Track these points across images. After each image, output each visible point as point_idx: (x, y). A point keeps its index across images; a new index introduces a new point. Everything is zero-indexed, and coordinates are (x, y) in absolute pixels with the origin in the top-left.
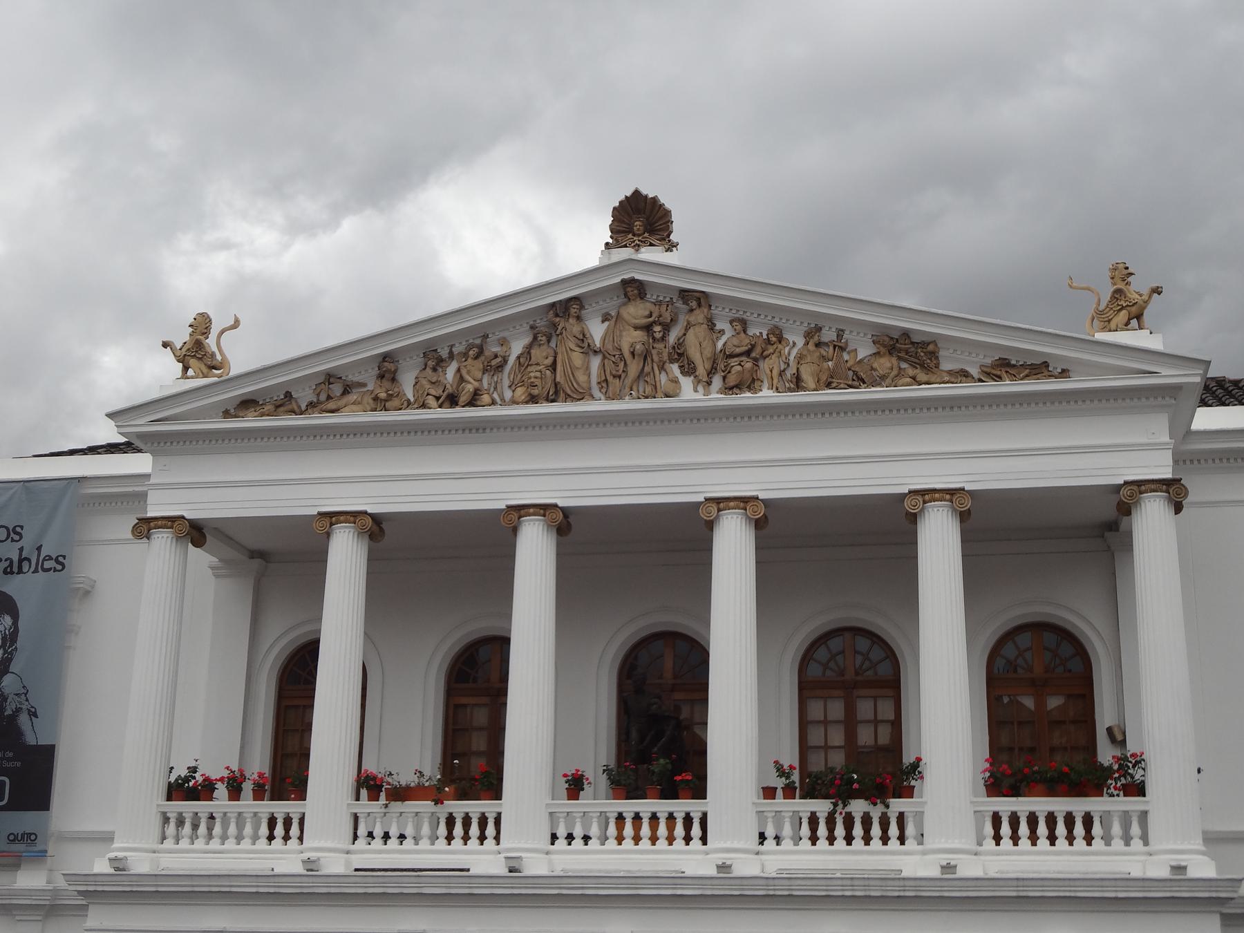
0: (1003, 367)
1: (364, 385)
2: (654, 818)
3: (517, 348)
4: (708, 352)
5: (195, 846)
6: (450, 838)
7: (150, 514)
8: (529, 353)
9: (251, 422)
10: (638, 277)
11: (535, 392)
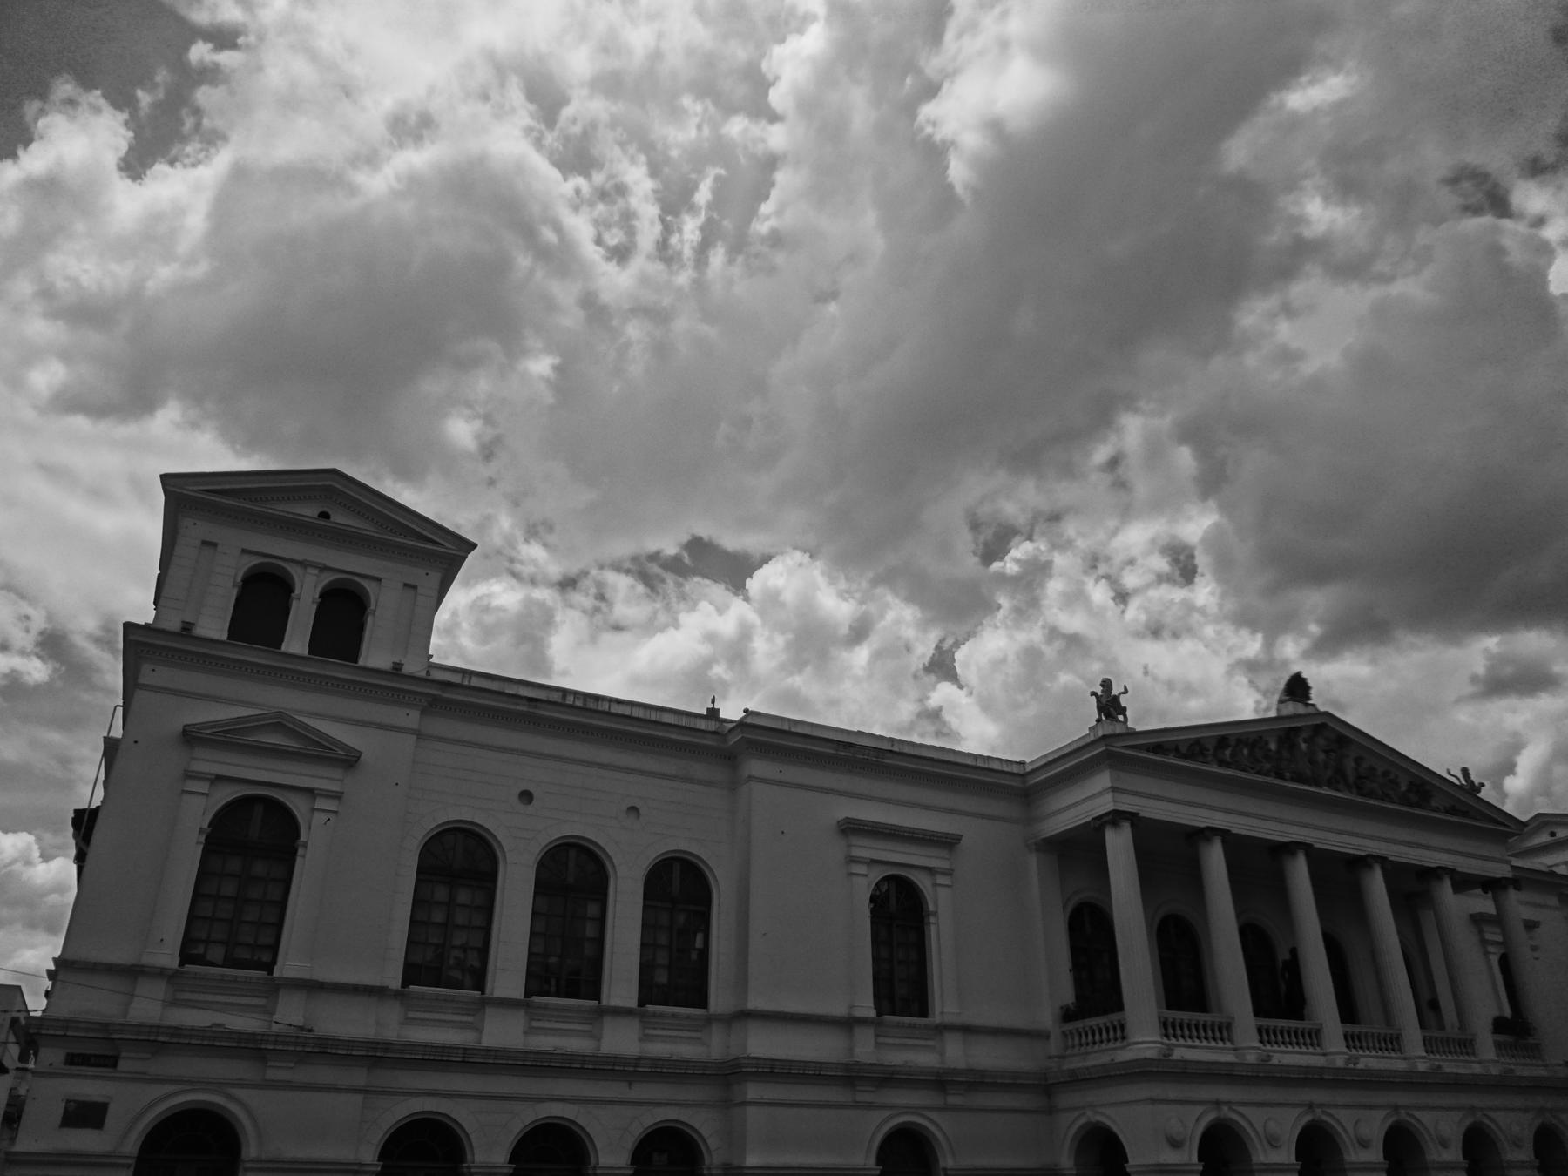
0: (1452, 811)
9: (1170, 760)
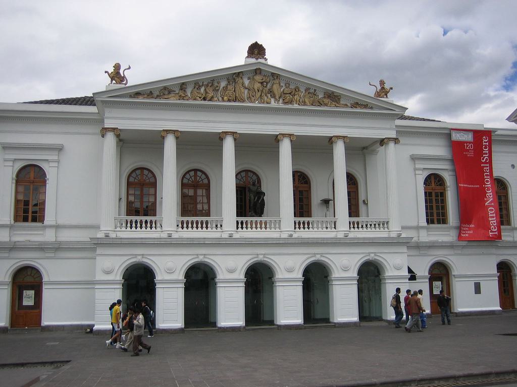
0: (356, 104)
1: (175, 91)
2: (131, 222)
3: (223, 84)
4: (280, 92)
5: (132, 230)
6: (182, 228)
7: (105, 127)
8: (227, 87)
10: (261, 68)
11: (230, 98)
